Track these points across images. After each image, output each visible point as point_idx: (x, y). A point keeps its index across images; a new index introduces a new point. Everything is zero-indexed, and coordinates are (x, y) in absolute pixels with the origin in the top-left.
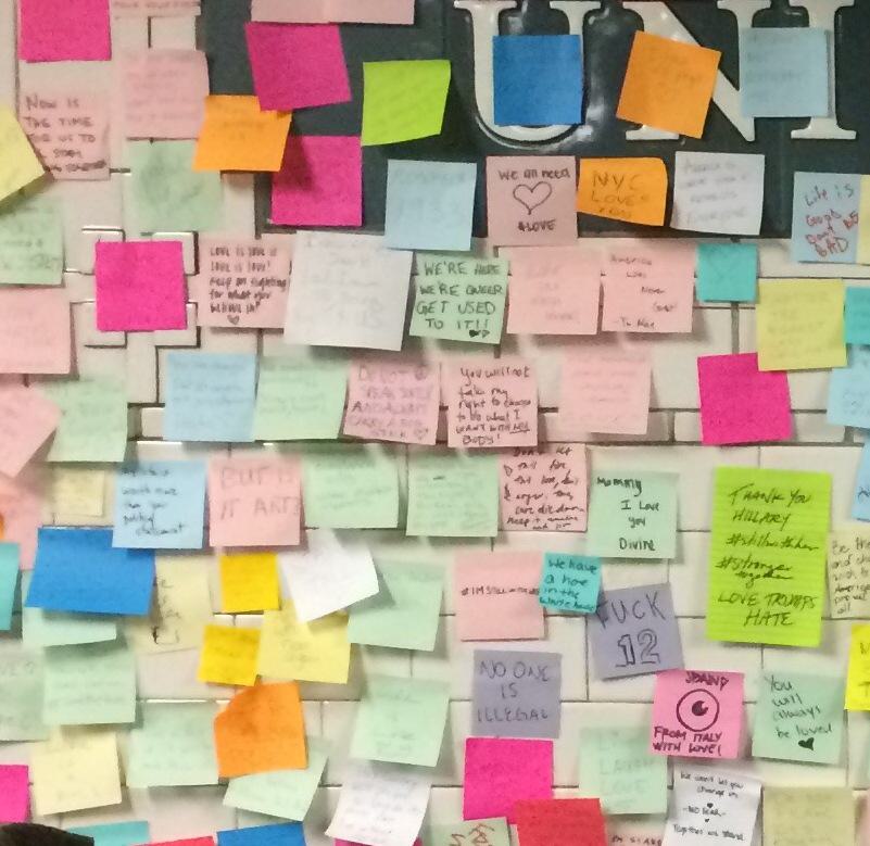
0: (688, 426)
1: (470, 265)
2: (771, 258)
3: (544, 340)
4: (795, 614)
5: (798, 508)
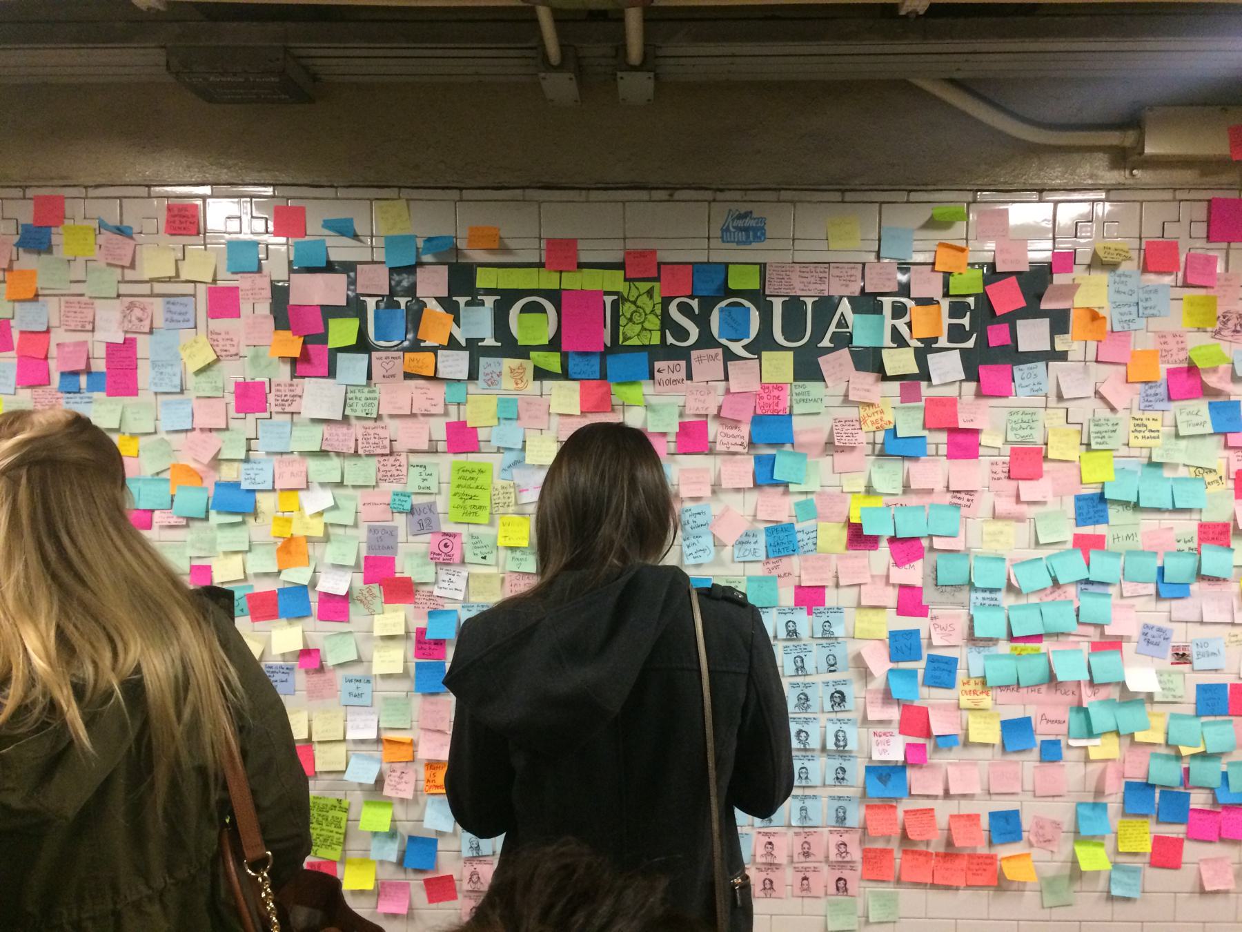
0: (442, 446)
1: (366, 390)
2: (472, 387)
3: (392, 416)
4: (480, 512)
5: (481, 475)
